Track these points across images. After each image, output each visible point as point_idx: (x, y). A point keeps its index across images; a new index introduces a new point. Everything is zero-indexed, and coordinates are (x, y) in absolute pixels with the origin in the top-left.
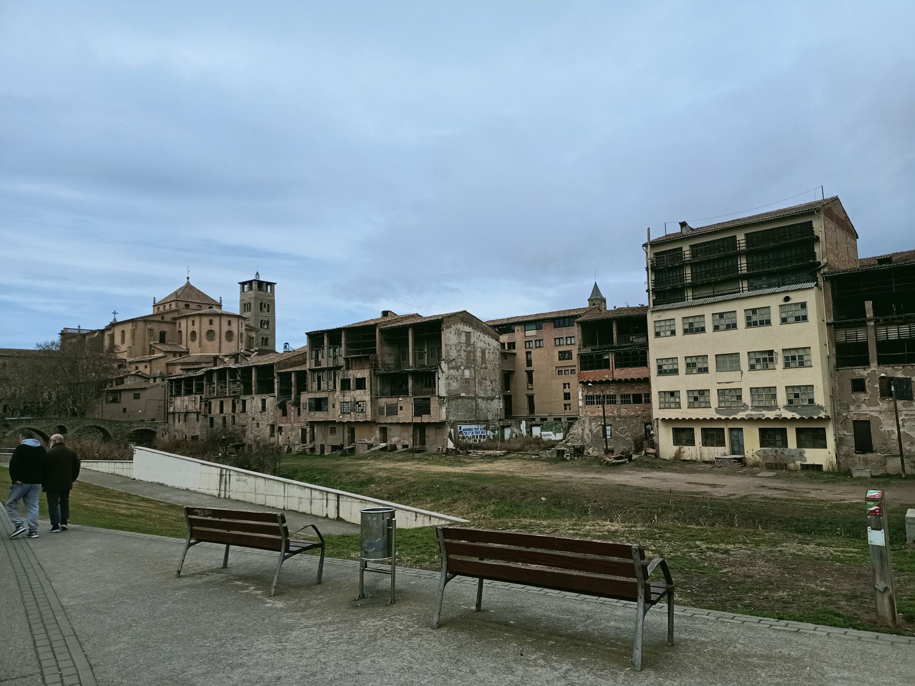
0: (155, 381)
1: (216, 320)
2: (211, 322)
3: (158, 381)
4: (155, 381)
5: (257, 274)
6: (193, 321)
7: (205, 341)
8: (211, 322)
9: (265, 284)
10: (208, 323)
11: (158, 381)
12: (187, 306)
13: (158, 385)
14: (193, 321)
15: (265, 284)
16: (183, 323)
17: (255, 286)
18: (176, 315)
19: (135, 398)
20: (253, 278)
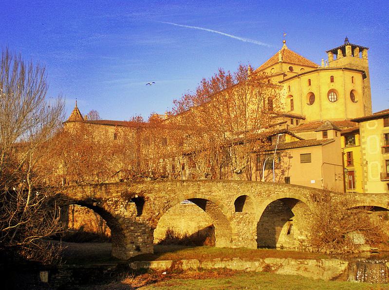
0: (325, 135)
1: (337, 74)
2: (332, 80)
3: (331, 134)
4: (325, 135)
5: (347, 40)
6: (310, 81)
7: (326, 103)
8: (332, 80)
9: (358, 48)
10: (329, 80)
11: (331, 134)
12: (291, 69)
13: (333, 141)
14: (310, 81)
15: (358, 48)
16: (294, 83)
17: (348, 50)
18: (281, 78)
19: (302, 161)
20: (343, 44)
